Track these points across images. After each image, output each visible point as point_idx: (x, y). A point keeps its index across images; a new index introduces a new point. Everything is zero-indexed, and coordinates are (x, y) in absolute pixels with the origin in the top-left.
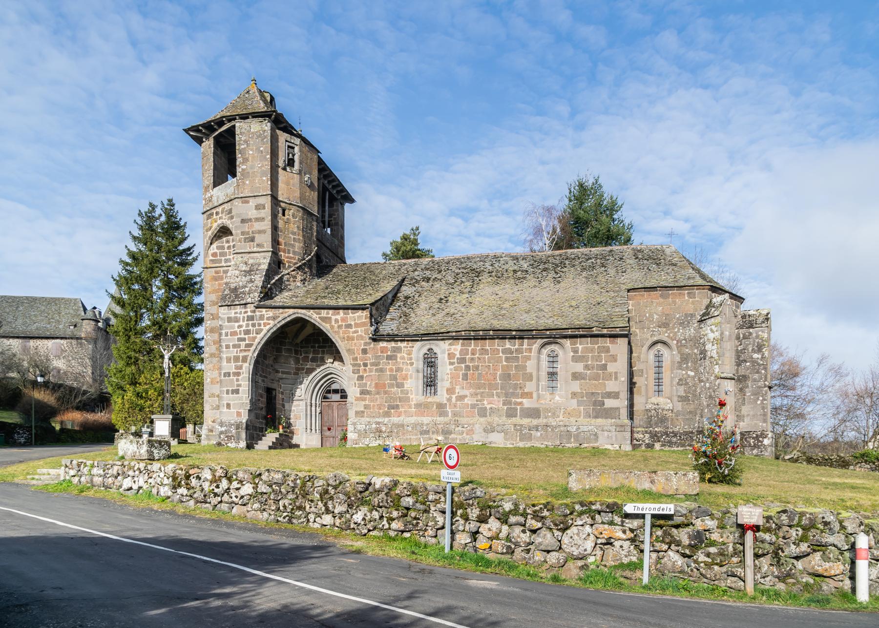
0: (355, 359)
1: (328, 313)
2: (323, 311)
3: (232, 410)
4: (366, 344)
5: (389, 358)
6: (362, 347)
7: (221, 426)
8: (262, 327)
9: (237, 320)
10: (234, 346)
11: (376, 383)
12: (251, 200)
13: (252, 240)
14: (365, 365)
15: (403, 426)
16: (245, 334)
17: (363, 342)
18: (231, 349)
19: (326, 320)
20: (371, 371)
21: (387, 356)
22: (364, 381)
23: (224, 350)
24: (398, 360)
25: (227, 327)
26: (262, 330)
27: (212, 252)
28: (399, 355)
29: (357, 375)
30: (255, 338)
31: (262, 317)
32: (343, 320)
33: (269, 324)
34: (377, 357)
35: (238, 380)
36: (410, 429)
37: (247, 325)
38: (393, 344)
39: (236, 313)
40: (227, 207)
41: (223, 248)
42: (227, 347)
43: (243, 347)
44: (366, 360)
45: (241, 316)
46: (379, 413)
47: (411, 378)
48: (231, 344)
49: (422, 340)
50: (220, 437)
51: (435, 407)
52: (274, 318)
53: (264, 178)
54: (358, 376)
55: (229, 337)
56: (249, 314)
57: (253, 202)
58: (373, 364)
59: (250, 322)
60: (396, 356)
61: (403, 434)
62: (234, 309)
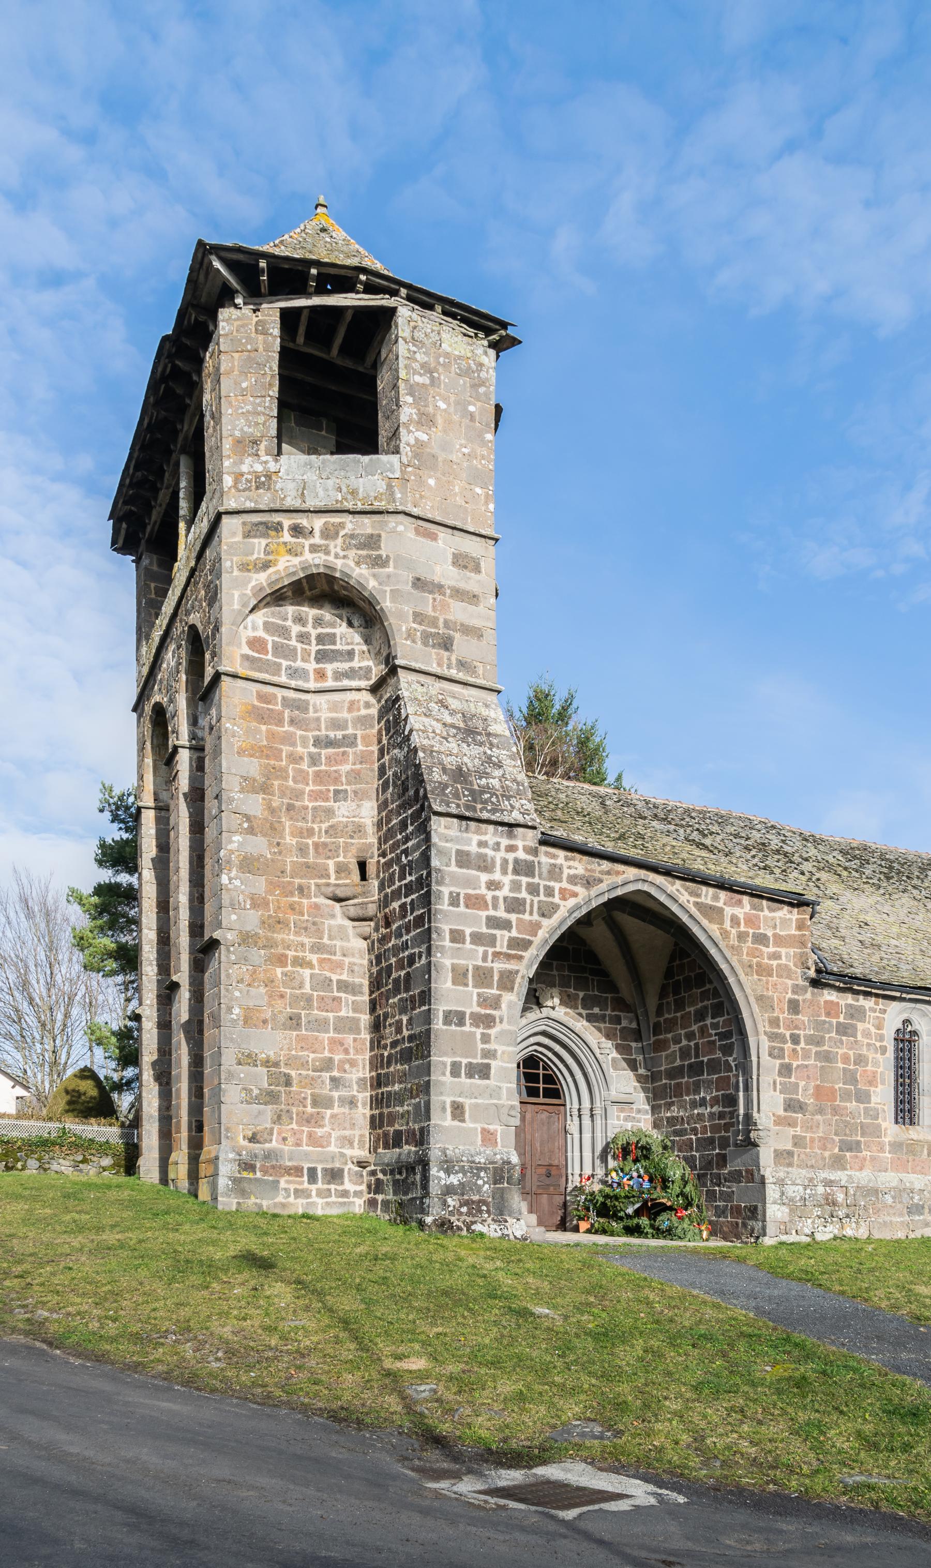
0: (775, 1022)
1: (715, 898)
2: (704, 888)
3: (469, 1124)
4: (796, 989)
5: (843, 1030)
6: (790, 995)
7: (448, 1172)
8: (556, 899)
9: (485, 865)
10: (477, 938)
11: (817, 1087)
12: (443, 534)
13: (447, 644)
14: (795, 1040)
15: (875, 1192)
16: (508, 910)
17: (790, 983)
18: (468, 945)
19: (713, 913)
20: (806, 1056)
21: (838, 1024)
22: (793, 1080)
23: (447, 943)
24: (859, 1037)
25: (456, 880)
26: (555, 908)
27: (251, 633)
28: (860, 1026)
29: (778, 1062)
30: (538, 926)
31: (555, 873)
32: (750, 921)
33: (575, 895)
34: (819, 1025)
35: (486, 1039)
36: (889, 1199)
37: (516, 886)
38: (849, 999)
39: (482, 844)
40: (367, 525)
41: (284, 632)
42: (457, 936)
43: (502, 946)
44: (796, 1028)
45: (499, 856)
46: (824, 1159)
47: (883, 1083)
48: (468, 931)
49: (904, 1000)
50: (445, 1203)
51: (926, 1152)
52: (588, 883)
53: (478, 490)
54: (782, 1065)
55: (462, 908)
56: (521, 855)
57: (446, 543)
58: (811, 1040)
59: (524, 880)
60: (855, 1028)
61: (877, 1212)
62: (478, 832)
